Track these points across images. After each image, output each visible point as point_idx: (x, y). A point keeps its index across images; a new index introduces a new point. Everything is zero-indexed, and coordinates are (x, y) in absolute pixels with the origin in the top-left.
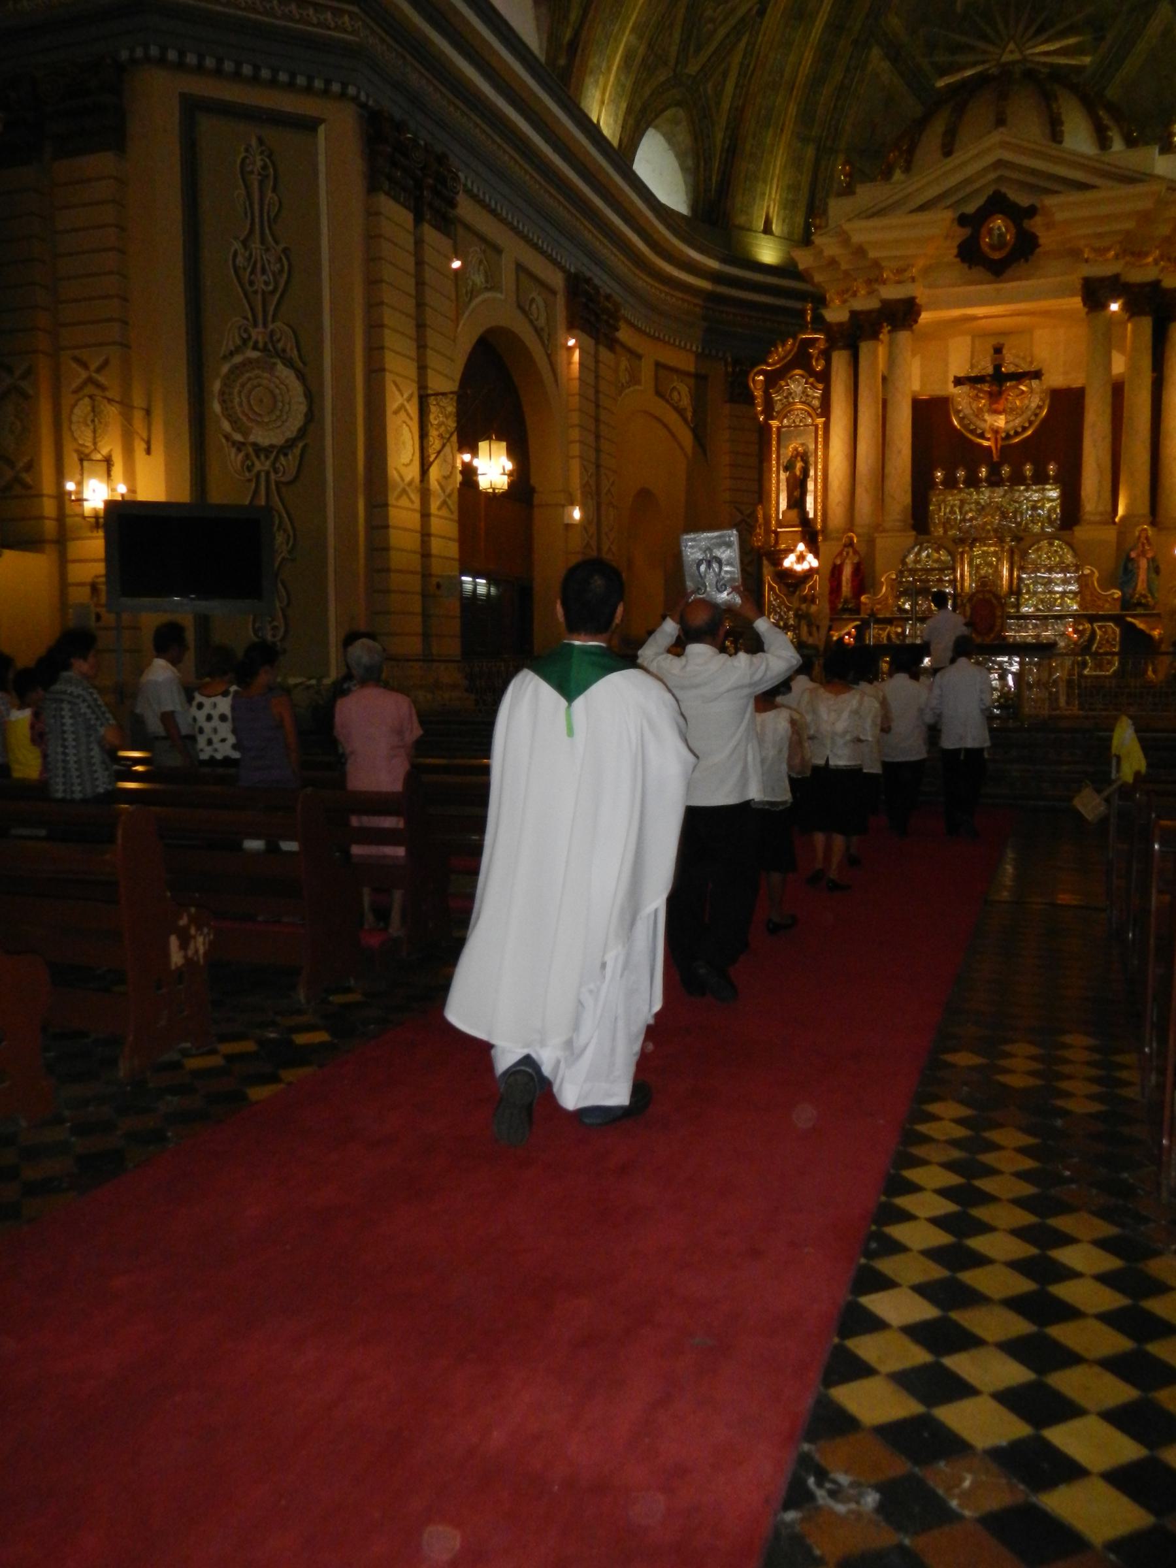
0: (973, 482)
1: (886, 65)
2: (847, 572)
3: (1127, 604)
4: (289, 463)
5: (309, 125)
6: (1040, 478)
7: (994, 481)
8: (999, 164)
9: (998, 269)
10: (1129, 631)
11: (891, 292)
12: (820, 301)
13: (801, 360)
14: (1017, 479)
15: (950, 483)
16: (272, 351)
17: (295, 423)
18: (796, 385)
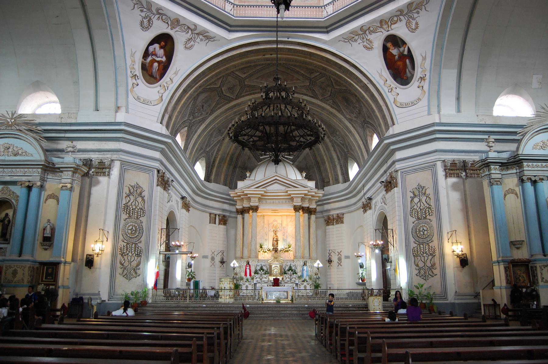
1: (249, 151)
8: (276, 179)
11: (253, 204)
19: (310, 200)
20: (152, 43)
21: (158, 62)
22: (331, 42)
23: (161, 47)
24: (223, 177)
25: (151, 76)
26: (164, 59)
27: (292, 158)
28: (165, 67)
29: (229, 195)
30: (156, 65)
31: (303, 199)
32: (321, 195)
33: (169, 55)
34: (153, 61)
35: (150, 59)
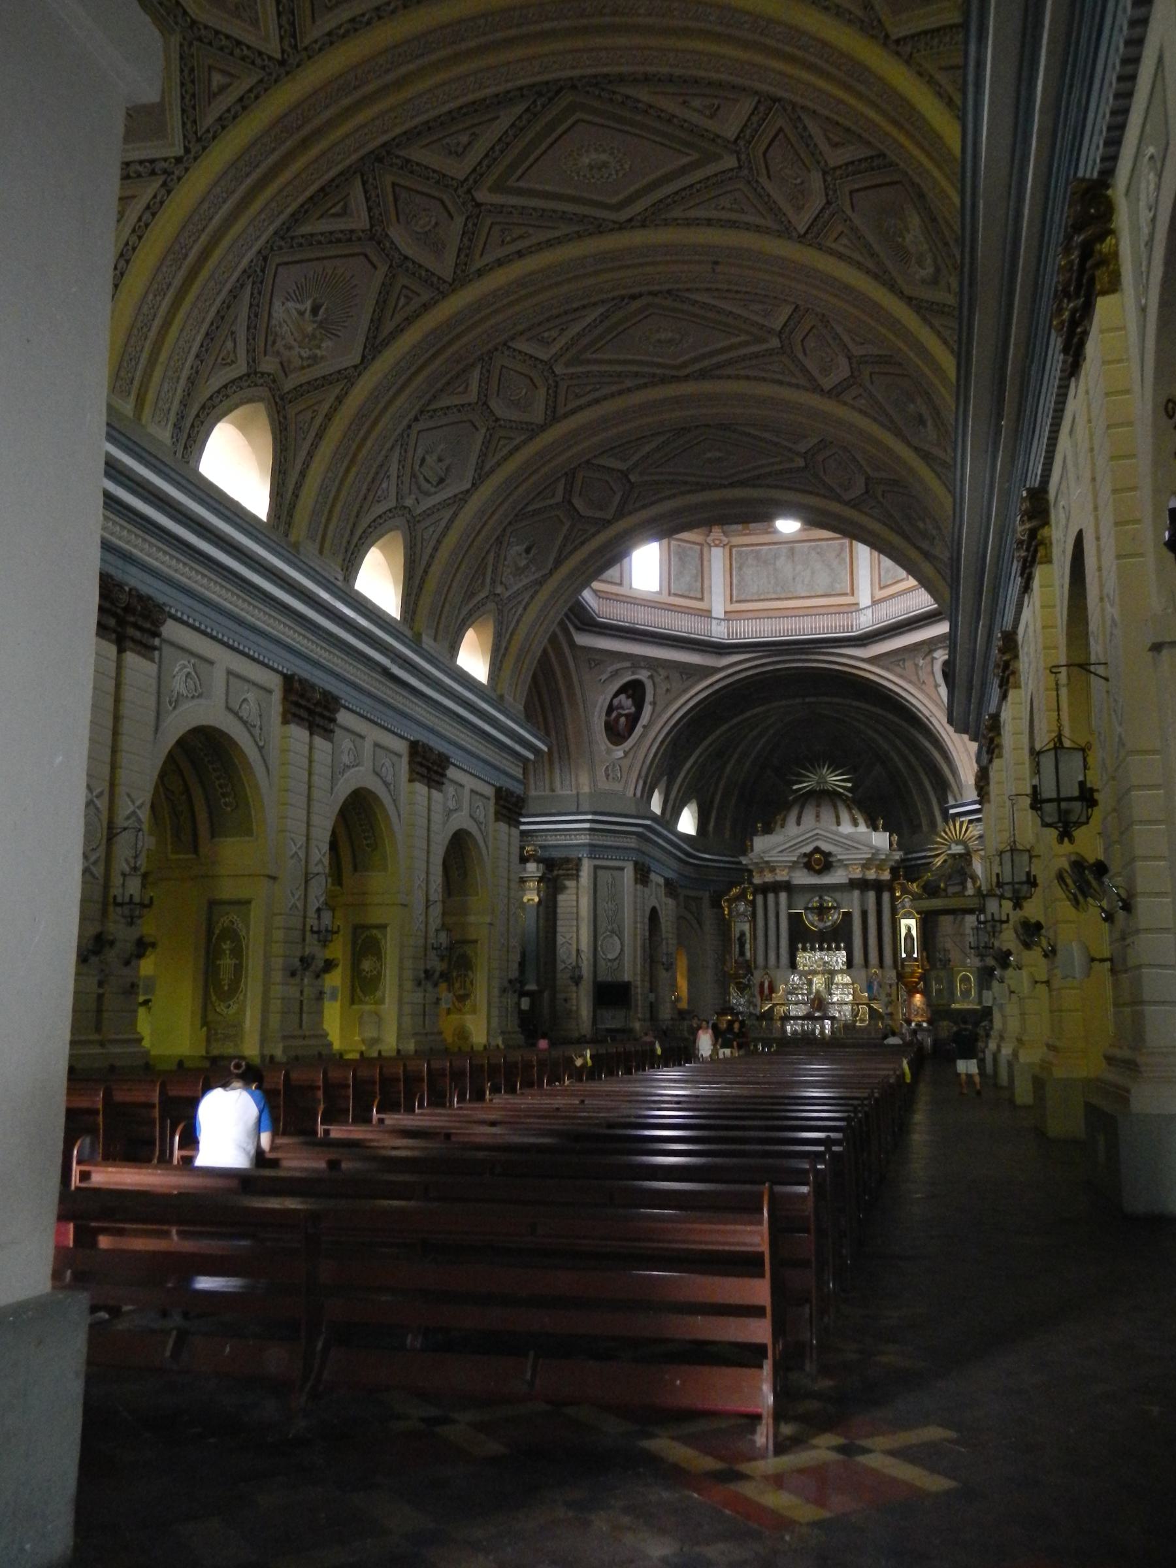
0: (813, 949)
2: (766, 985)
3: (871, 999)
4: (616, 963)
5: (622, 869)
6: (838, 948)
7: (821, 949)
9: (819, 873)
10: (871, 1008)
12: (750, 872)
13: (742, 896)
14: (829, 949)
15: (804, 950)
16: (613, 932)
17: (618, 951)
18: (742, 906)
19: (880, 868)
20: (616, 695)
21: (626, 716)
22: (871, 660)
23: (628, 697)
24: (728, 824)
25: (619, 734)
26: (633, 710)
27: (850, 785)
28: (634, 720)
29: (740, 863)
30: (623, 720)
31: (866, 866)
32: (897, 857)
33: (639, 706)
34: (620, 715)
35: (614, 714)
